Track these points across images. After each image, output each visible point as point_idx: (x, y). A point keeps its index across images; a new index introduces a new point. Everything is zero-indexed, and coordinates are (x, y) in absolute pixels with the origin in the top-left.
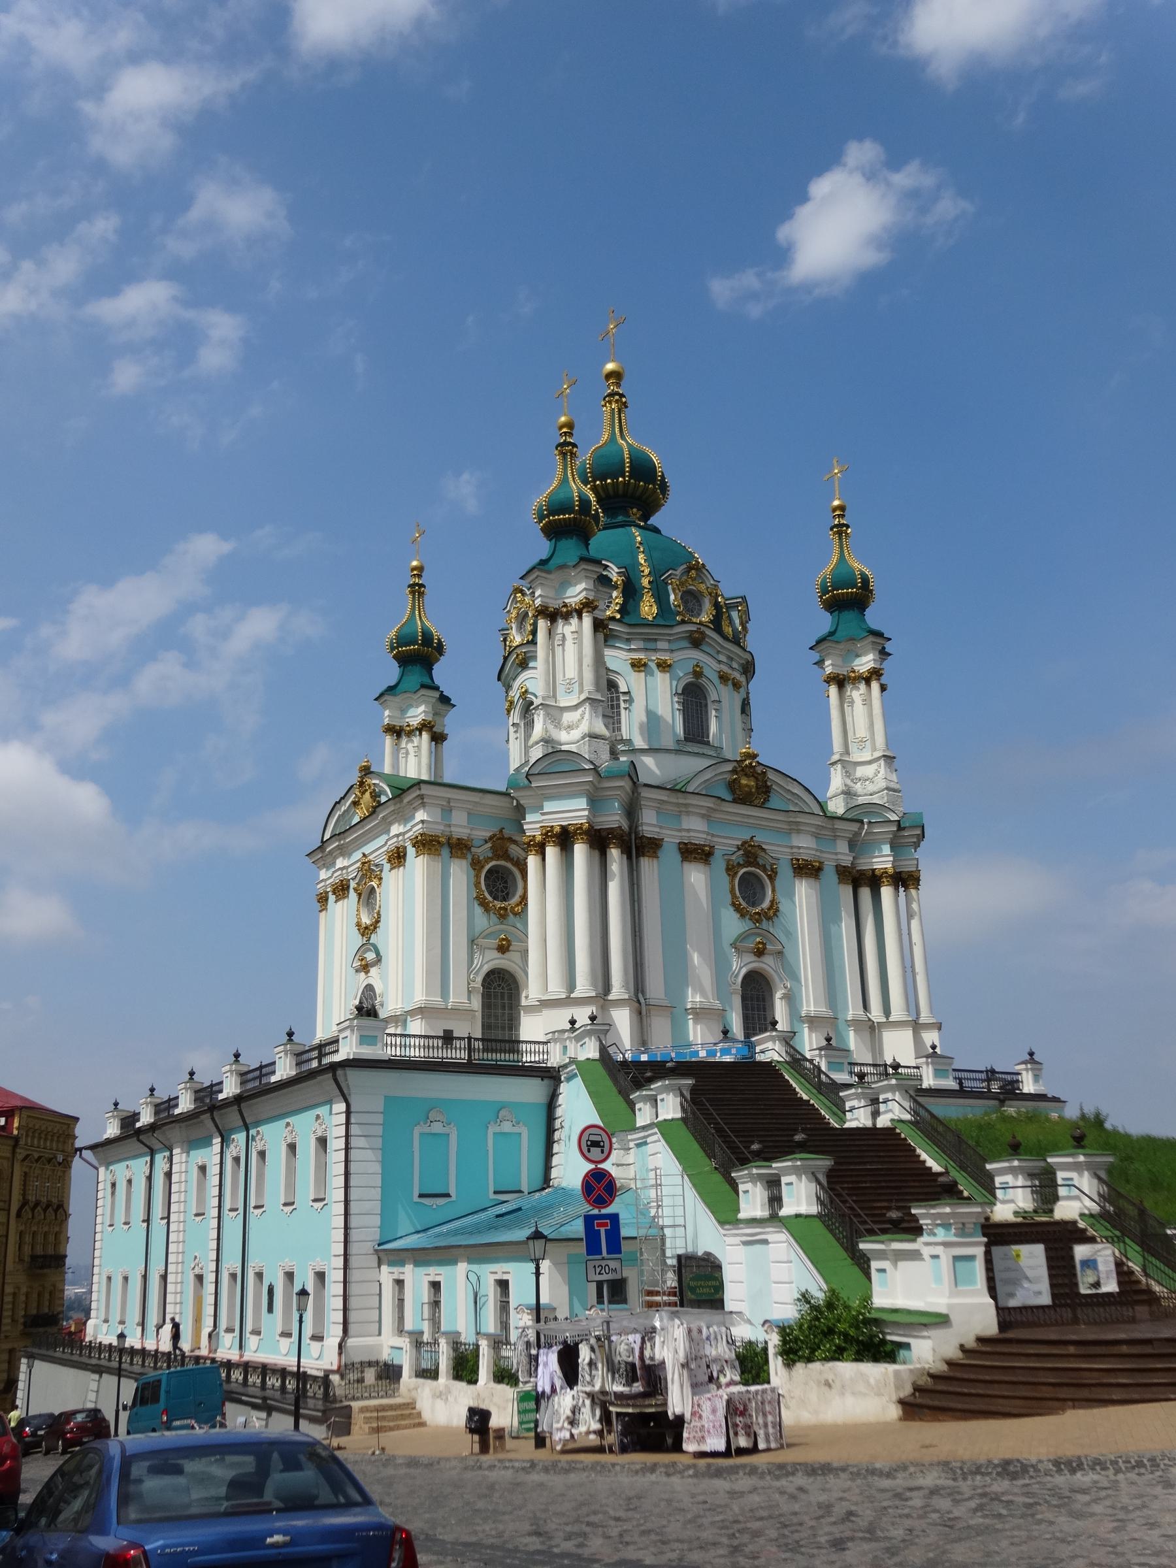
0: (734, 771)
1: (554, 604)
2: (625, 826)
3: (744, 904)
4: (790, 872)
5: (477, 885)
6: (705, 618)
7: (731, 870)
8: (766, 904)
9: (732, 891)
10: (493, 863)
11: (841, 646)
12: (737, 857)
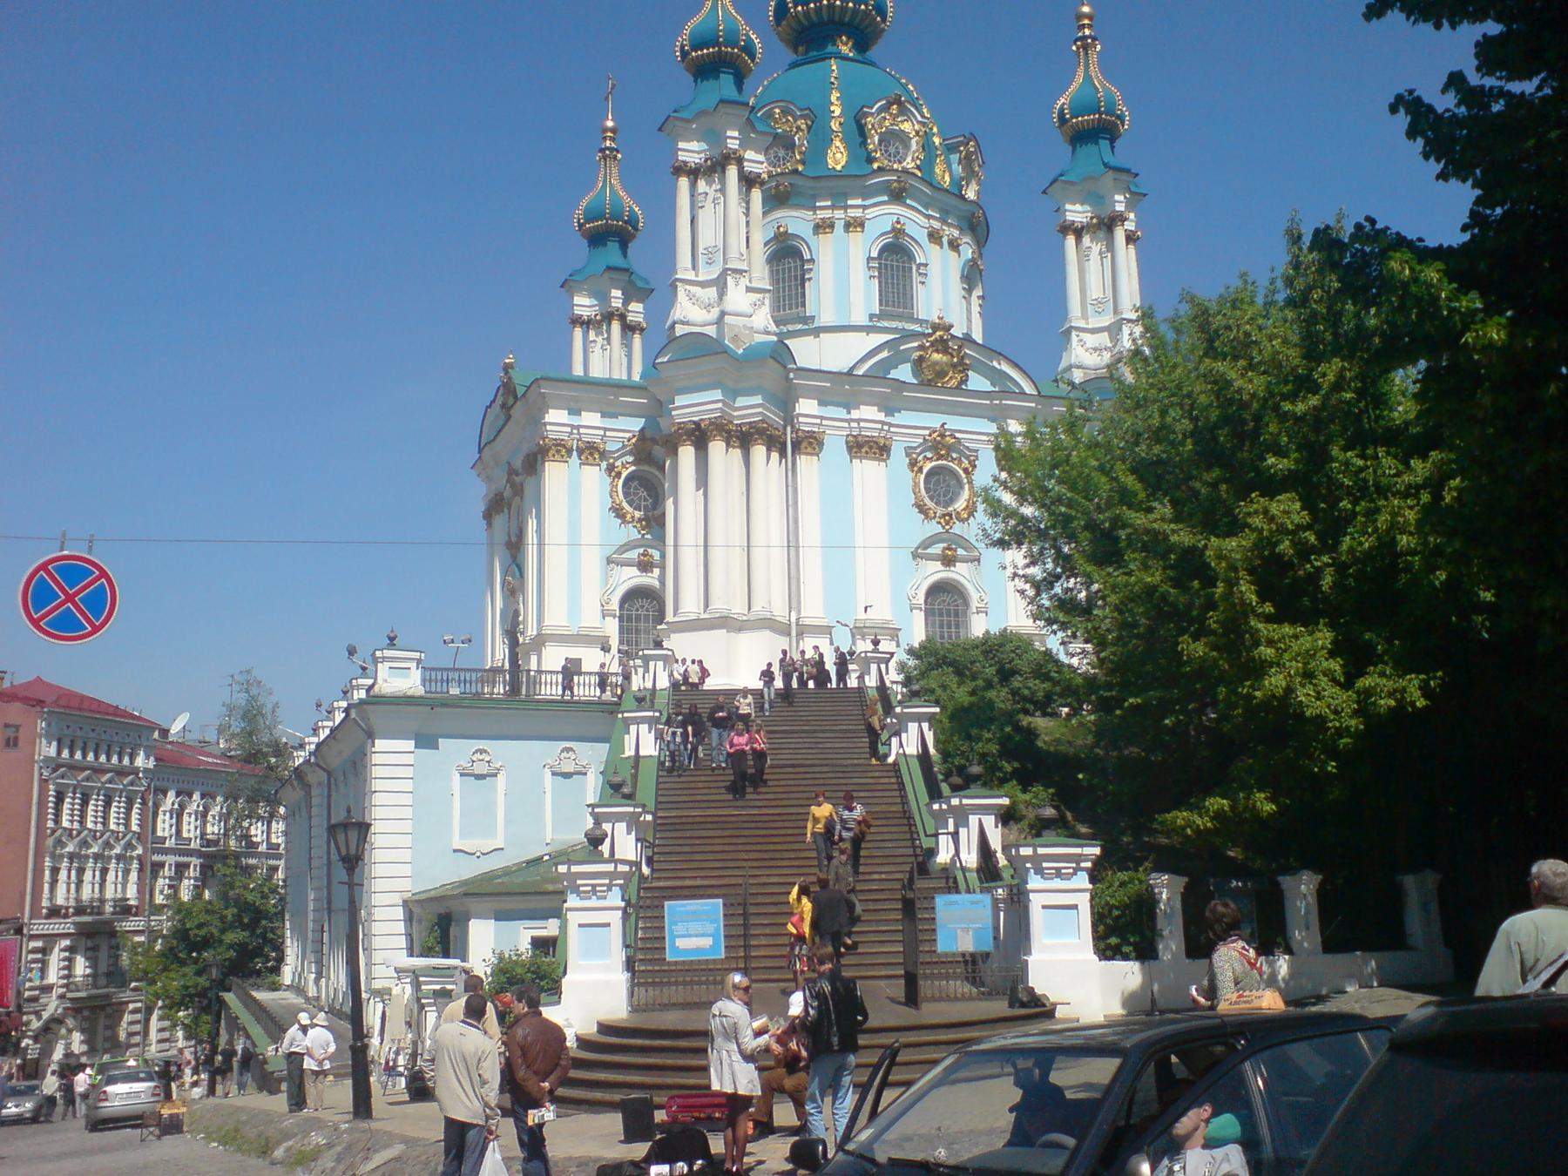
0: (921, 347)
2: (776, 418)
3: (930, 504)
5: (613, 492)
6: (909, 164)
8: (960, 504)
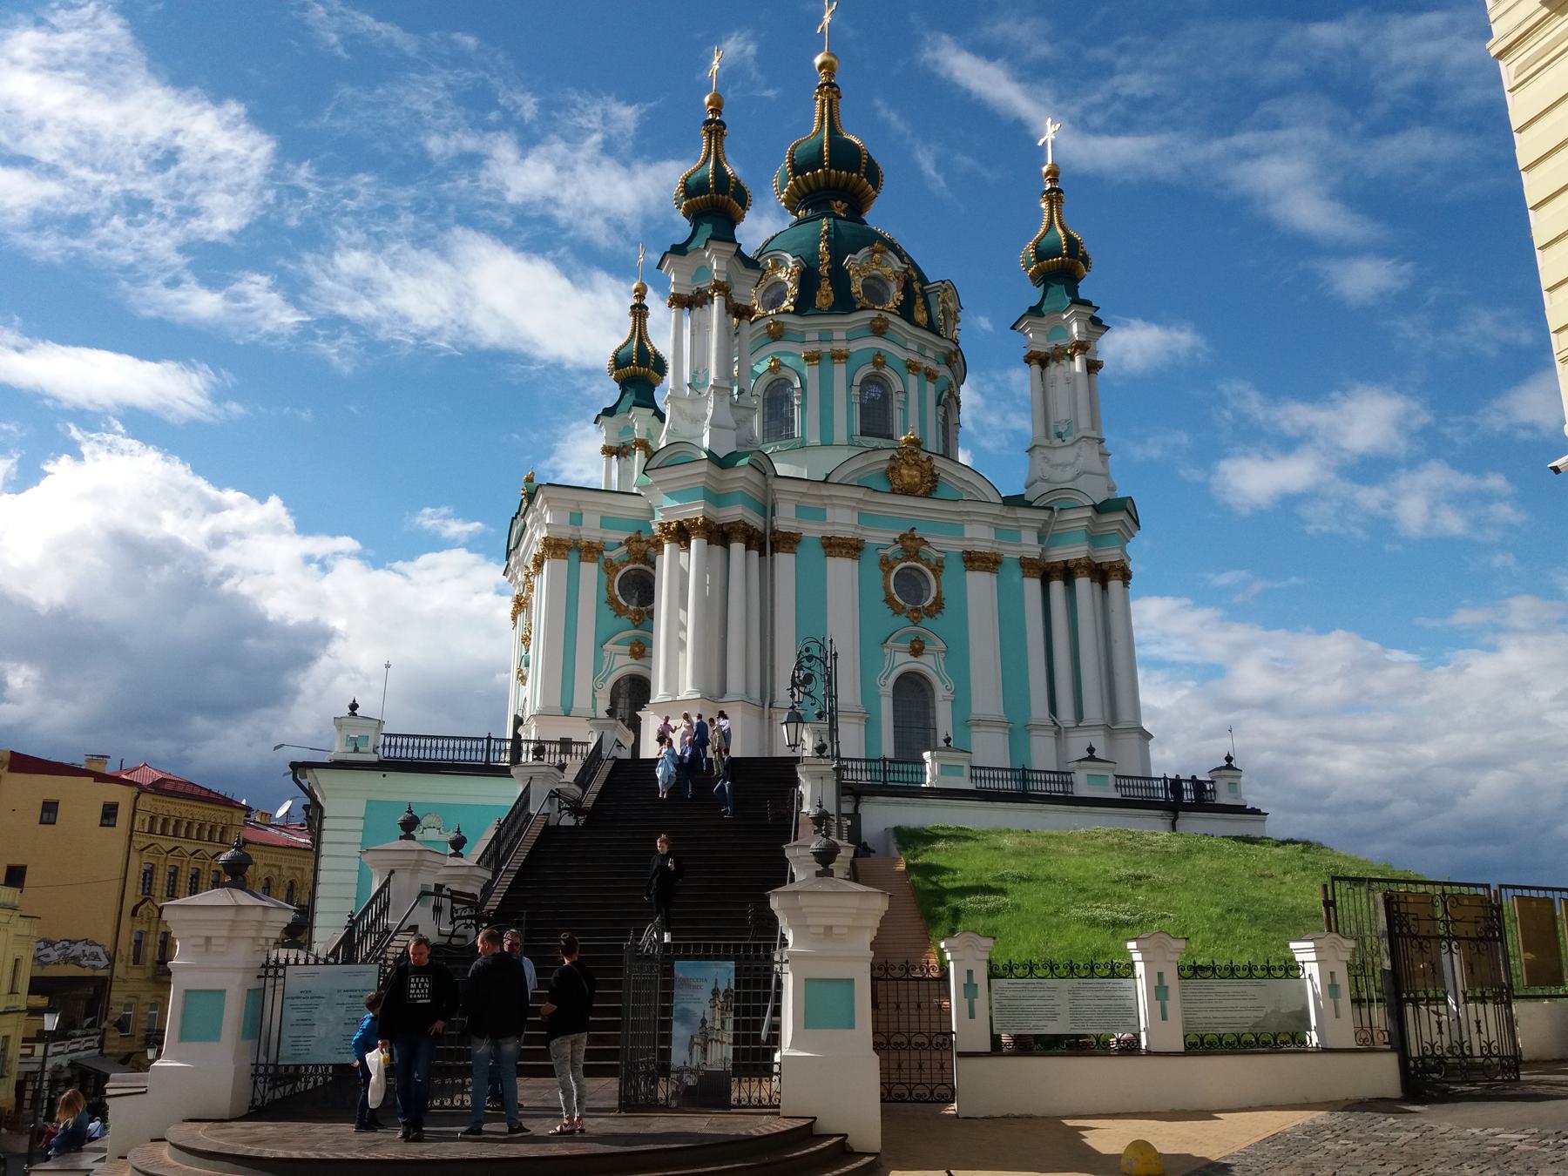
0: (892, 458)
1: (688, 291)
2: (755, 521)
4: (962, 566)
7: (886, 564)
9: (886, 588)
10: (630, 566)
11: (1044, 321)
12: (893, 551)
